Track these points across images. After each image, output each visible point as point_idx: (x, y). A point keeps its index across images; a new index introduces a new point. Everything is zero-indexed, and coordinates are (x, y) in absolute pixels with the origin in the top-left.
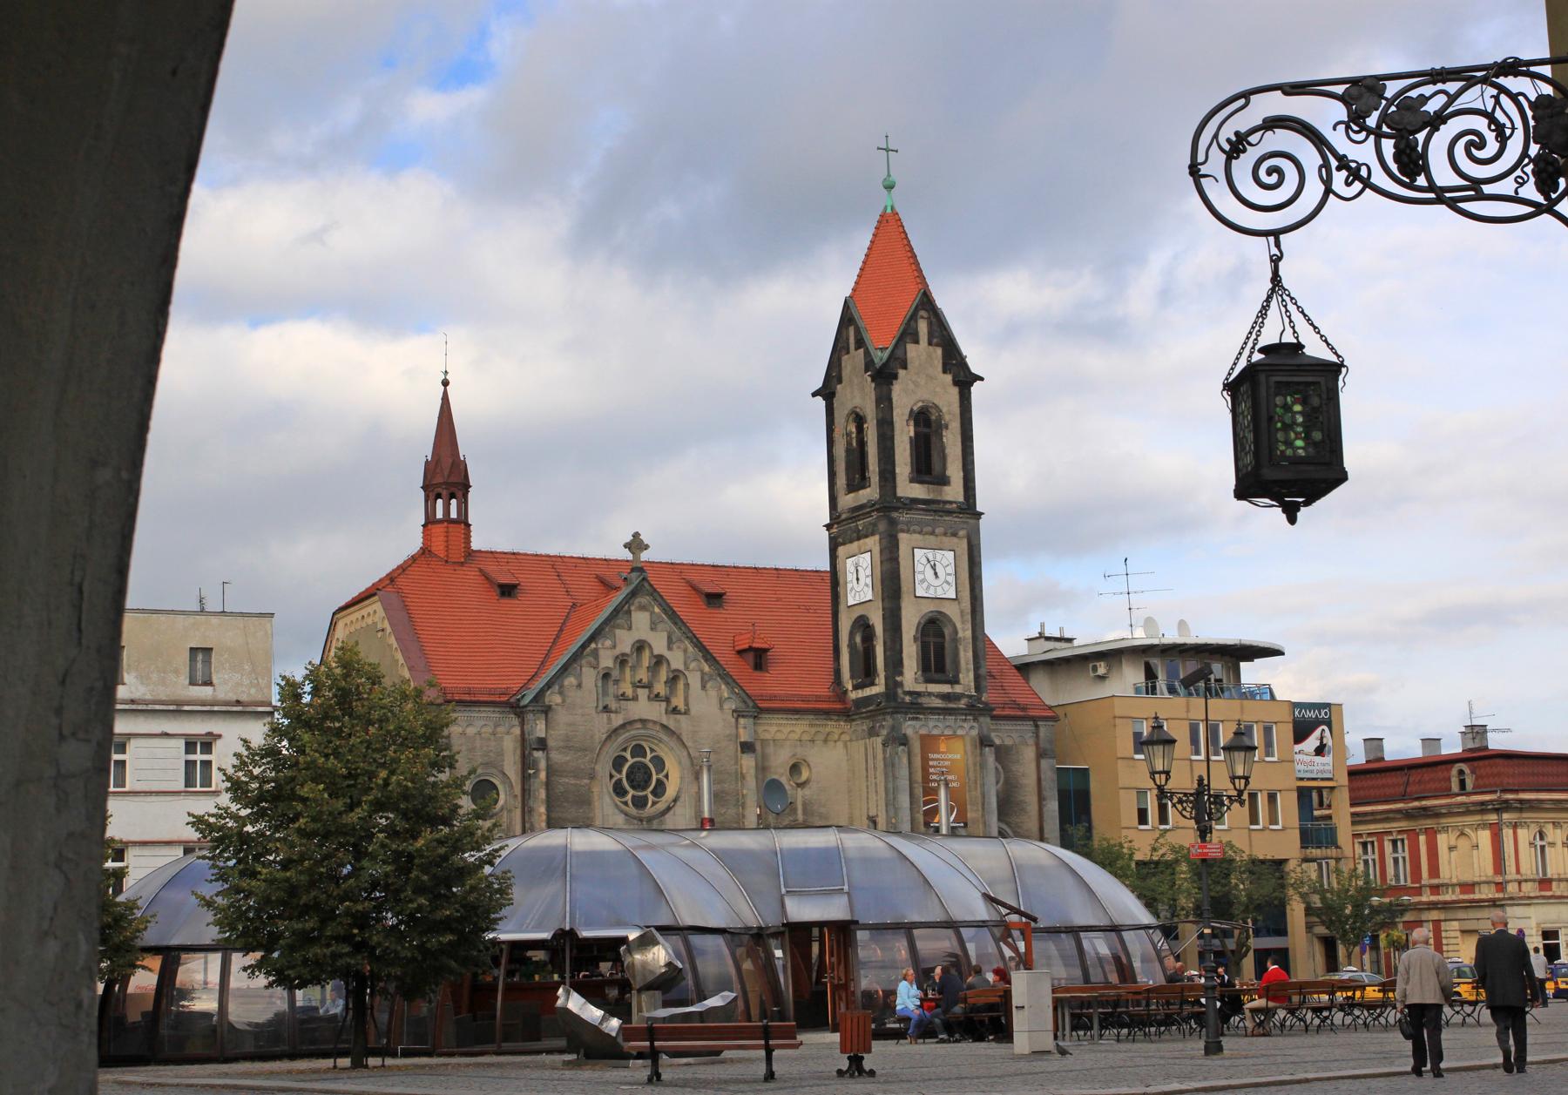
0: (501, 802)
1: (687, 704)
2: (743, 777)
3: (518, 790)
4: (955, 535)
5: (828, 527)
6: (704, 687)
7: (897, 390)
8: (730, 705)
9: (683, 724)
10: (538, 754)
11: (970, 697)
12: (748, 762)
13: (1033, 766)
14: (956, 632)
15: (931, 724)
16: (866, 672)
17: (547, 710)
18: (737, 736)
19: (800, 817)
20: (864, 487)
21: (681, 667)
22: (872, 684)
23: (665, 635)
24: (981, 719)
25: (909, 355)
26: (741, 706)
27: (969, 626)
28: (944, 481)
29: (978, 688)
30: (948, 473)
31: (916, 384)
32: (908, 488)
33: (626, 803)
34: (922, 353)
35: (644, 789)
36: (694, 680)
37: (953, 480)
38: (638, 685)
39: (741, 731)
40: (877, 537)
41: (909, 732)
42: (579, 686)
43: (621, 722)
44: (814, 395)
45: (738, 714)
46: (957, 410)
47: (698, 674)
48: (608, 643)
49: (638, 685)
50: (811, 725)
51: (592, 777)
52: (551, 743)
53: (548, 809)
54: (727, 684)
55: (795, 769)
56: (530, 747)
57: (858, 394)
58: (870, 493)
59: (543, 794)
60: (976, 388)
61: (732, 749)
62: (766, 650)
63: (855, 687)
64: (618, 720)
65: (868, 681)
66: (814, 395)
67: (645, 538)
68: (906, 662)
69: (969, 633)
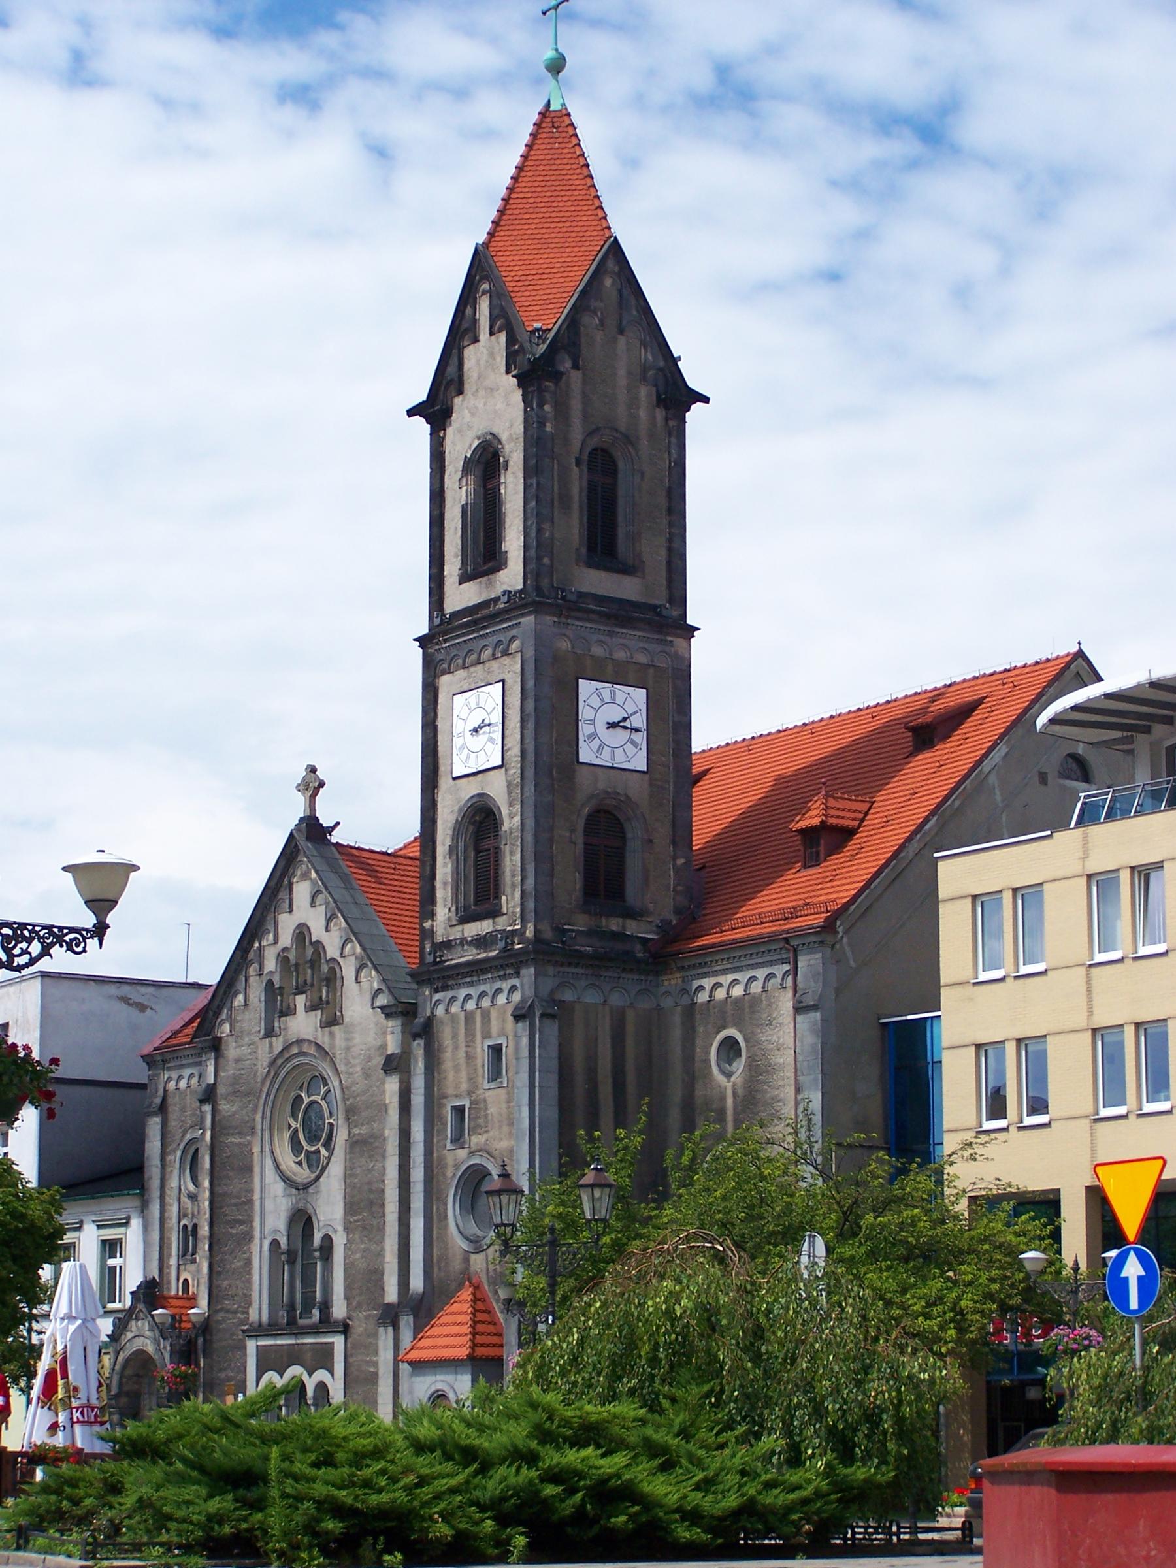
4: (506, 653)
17: (216, 1046)
21: (336, 955)
25: (467, 366)
33: (299, 1163)
47: (353, 958)
52: (221, 1090)
68: (439, 894)
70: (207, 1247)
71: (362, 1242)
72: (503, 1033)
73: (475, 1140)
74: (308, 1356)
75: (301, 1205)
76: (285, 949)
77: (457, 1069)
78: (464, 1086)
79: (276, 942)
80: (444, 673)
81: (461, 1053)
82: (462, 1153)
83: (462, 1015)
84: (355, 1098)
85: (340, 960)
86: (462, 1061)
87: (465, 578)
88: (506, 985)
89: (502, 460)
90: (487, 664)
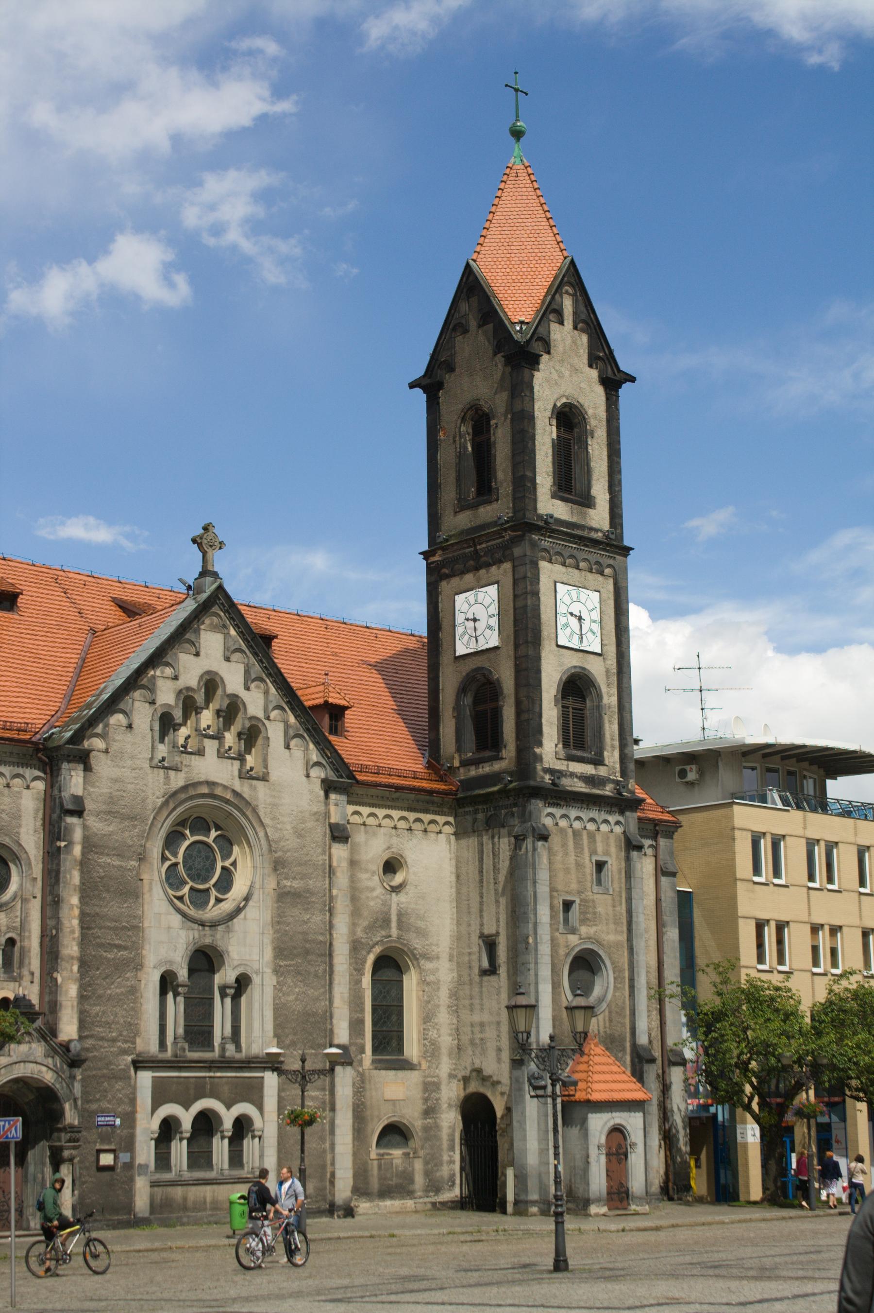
0: (13, 887)
1: (266, 767)
2: (331, 871)
3: (37, 870)
4: (602, 573)
5: (426, 555)
6: (288, 747)
7: (539, 378)
8: (318, 773)
9: (260, 794)
10: (70, 820)
11: (617, 783)
12: (339, 852)
13: (652, 881)
14: (600, 697)
15: (573, 813)
16: (488, 738)
18: (327, 814)
19: (394, 932)
20: (490, 502)
21: (261, 715)
22: (498, 758)
23: (241, 668)
24: (628, 814)
26: (332, 776)
27: (615, 691)
28: (586, 501)
29: (624, 772)
30: (594, 492)
31: (561, 376)
32: (549, 505)
33: (181, 899)
34: (565, 336)
35: (206, 880)
36: (275, 732)
37: (598, 501)
38: (204, 735)
39: (332, 808)
40: (507, 566)
41: (548, 822)
42: (130, 726)
43: (181, 783)
44: (412, 386)
45: (329, 787)
46: (603, 415)
47: (281, 726)
48: (168, 671)
49: (204, 735)
50: (410, 809)
51: (142, 858)
52: (89, 805)
53: (84, 899)
54: (317, 744)
55: (391, 866)
56: (59, 813)
57: (477, 382)
58: (498, 510)
59: (75, 877)
60: (626, 390)
61: (320, 833)
62: (347, 708)
63: (465, 764)
64: (178, 780)
65: (487, 754)
66: (412, 386)
67: (221, 532)
68: (545, 729)
69: (614, 700)
70: (75, 968)
71: (296, 986)
72: (606, 853)
73: (584, 930)
74: (225, 1090)
75: (208, 941)
76: (188, 689)
77: (567, 871)
78: (574, 886)
79: (176, 678)
80: (543, 559)
81: (572, 858)
82: (573, 939)
83: (570, 831)
84: (286, 852)
85: (266, 722)
86: (573, 866)
87: (554, 496)
88: (612, 819)
89: (588, 427)
90: (583, 573)
